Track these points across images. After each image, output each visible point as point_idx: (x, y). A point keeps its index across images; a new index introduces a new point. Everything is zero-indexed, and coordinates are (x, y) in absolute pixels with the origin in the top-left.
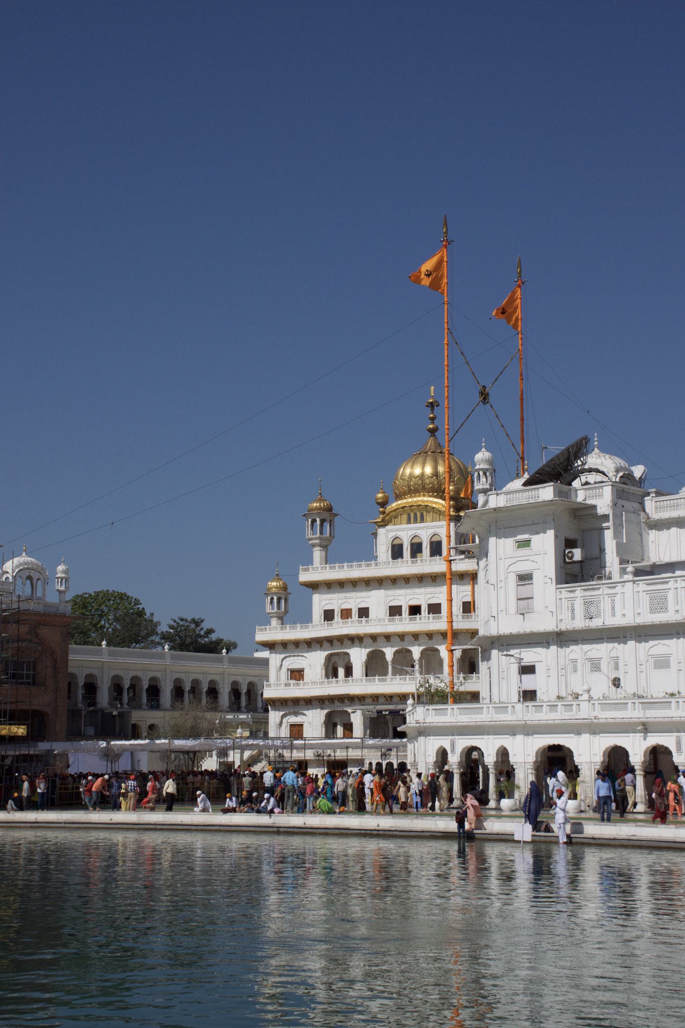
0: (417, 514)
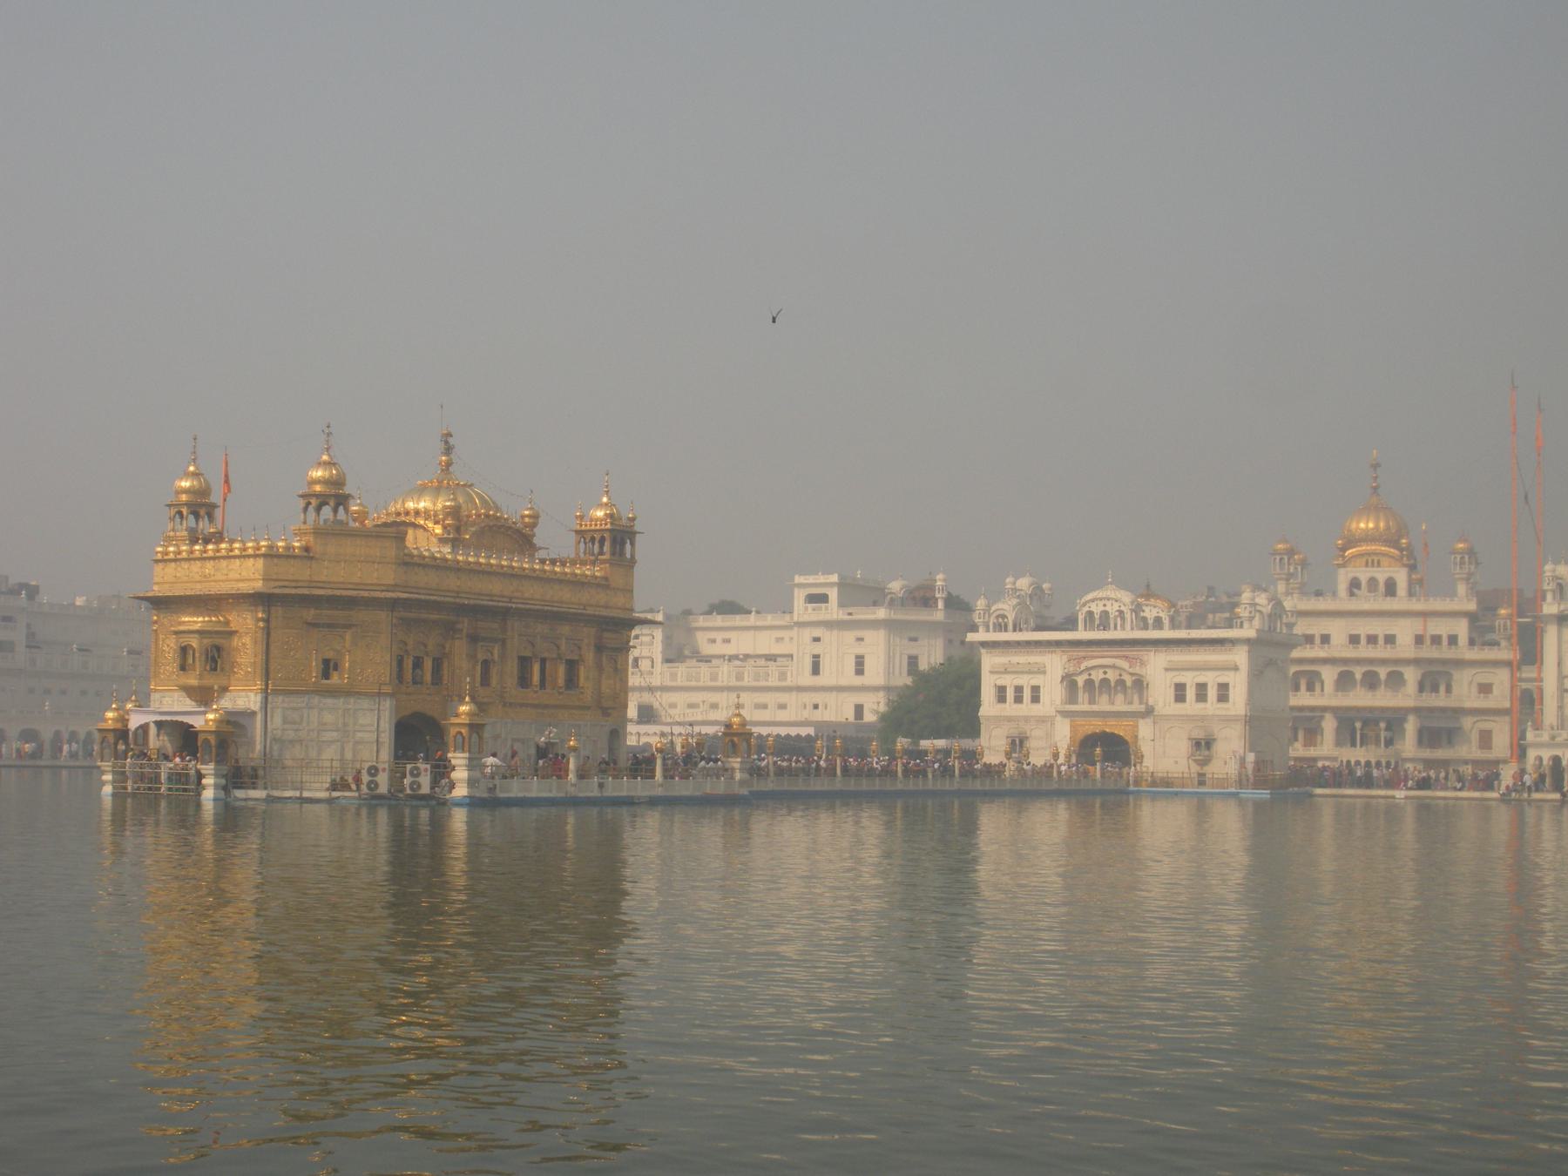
0: (1372, 560)
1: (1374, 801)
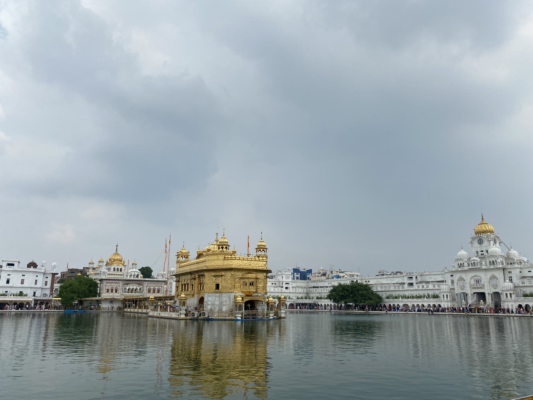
1: (93, 313)
